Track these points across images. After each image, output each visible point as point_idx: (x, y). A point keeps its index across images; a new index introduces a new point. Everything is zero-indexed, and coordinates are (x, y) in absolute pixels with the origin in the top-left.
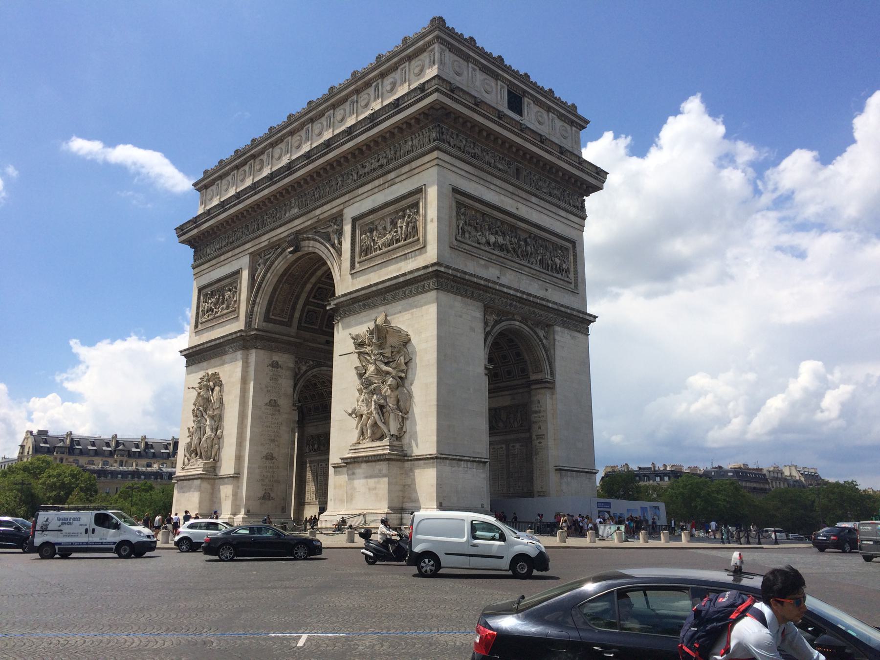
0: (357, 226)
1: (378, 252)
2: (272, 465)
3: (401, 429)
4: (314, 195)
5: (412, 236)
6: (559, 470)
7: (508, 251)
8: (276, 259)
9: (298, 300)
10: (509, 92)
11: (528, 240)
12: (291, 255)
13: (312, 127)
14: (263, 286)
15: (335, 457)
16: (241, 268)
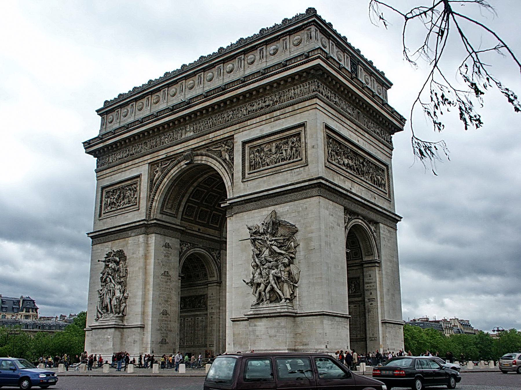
0: (246, 147)
1: (266, 167)
2: (167, 319)
3: (291, 295)
4: (208, 123)
5: (295, 157)
6: (384, 323)
7: (354, 170)
8: (172, 169)
9: (183, 199)
10: (351, 61)
11: (365, 163)
12: (185, 166)
13: (204, 75)
14: (160, 187)
15: (230, 314)
16: (141, 174)
